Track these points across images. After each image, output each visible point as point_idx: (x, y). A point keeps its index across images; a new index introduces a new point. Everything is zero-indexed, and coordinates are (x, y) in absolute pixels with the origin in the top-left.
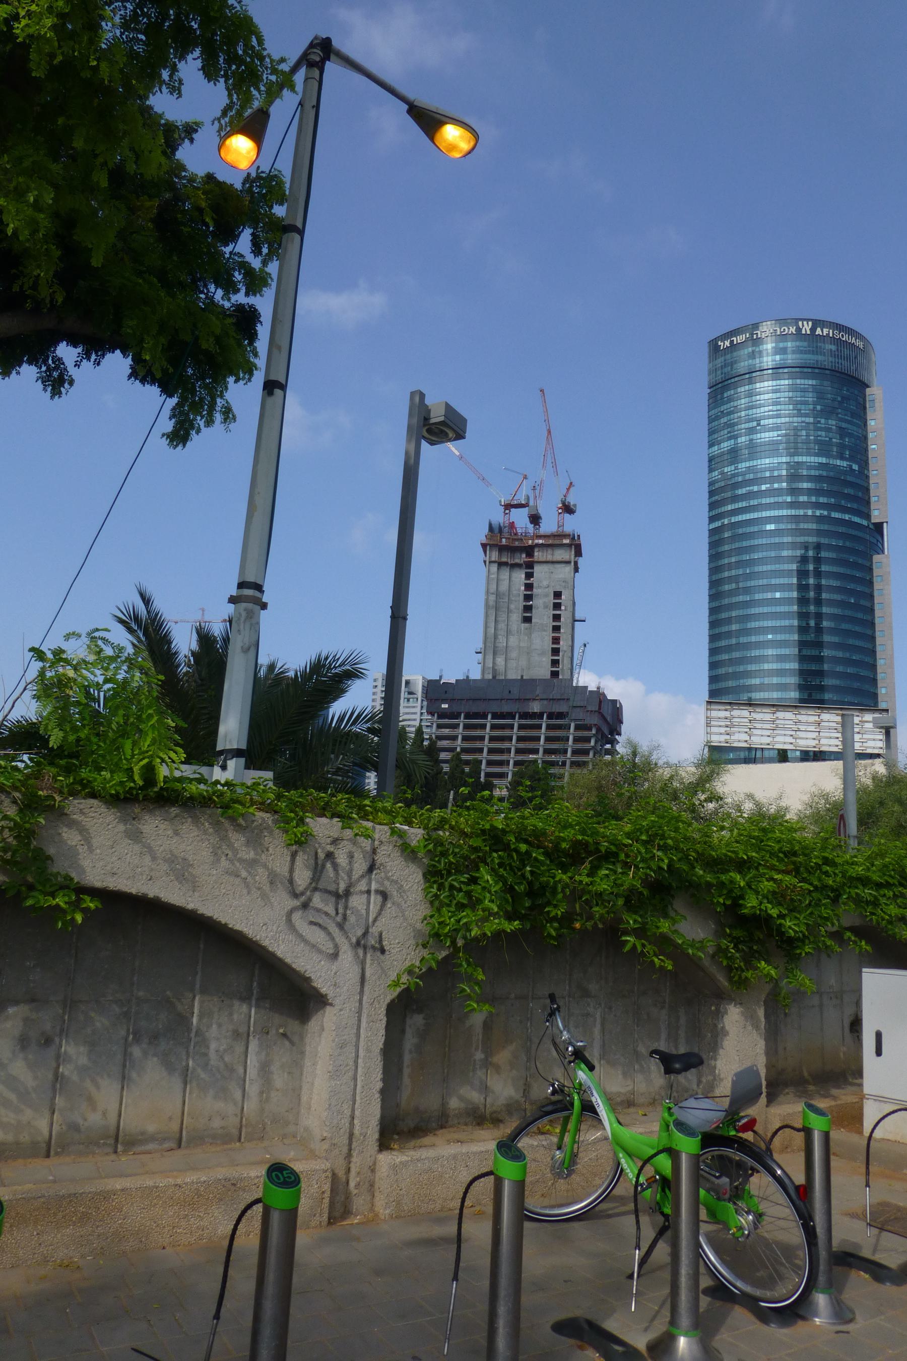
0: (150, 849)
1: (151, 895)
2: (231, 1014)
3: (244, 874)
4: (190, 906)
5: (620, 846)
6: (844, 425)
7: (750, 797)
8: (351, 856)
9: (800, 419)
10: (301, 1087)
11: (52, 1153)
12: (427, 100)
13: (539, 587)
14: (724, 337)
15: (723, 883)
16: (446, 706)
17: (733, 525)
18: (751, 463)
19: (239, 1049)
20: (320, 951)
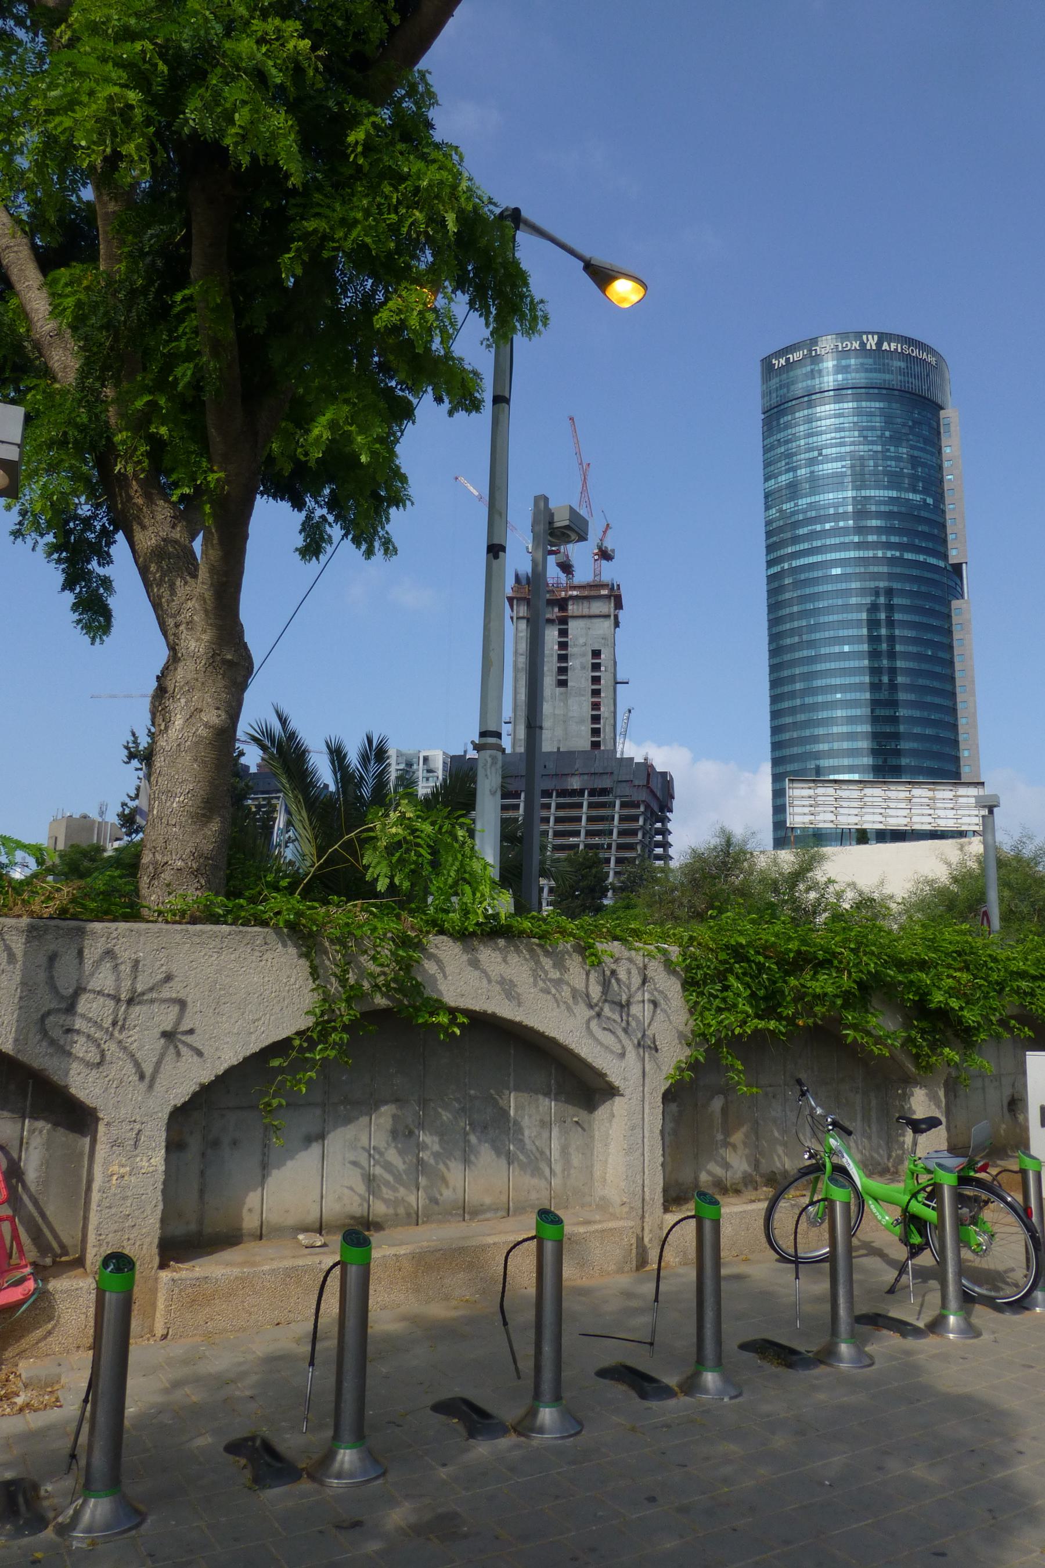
0: (484, 972)
1: (489, 1012)
2: (537, 1107)
3: (553, 991)
4: (518, 1019)
5: (834, 955)
6: (916, 453)
7: (852, 885)
8: (629, 972)
9: (866, 448)
10: (592, 1165)
11: (420, 1221)
12: (600, 258)
13: (575, 645)
14: (779, 354)
15: (912, 982)
17: (794, 570)
18: (813, 499)
19: (545, 1135)
20: (612, 1052)
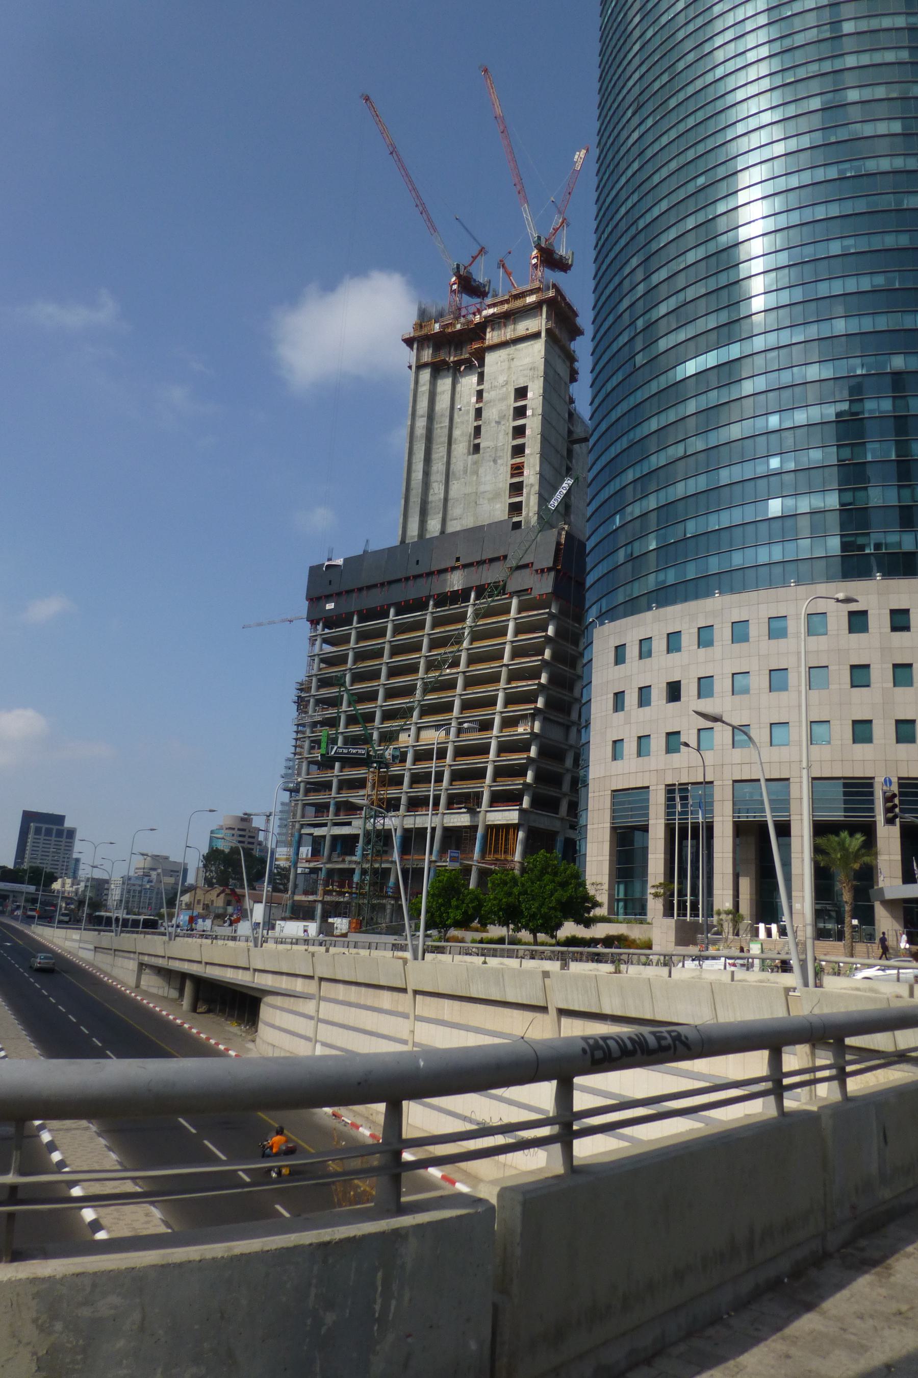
13: (493, 388)
16: (330, 606)
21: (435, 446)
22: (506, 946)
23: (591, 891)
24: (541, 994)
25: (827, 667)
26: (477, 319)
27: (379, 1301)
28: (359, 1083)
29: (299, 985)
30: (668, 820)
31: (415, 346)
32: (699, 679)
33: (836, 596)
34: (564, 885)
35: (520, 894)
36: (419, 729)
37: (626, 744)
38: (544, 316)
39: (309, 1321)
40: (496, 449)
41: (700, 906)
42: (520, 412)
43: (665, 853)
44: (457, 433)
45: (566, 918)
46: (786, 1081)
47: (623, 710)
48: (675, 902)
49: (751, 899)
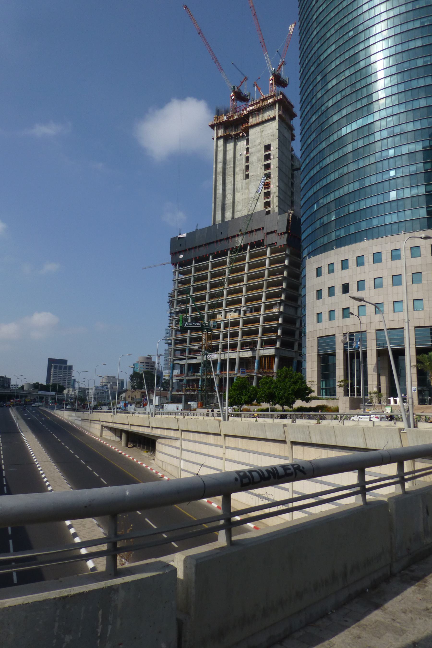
13: (254, 146)
16: (181, 256)
21: (227, 177)
22: (270, 413)
23: (309, 385)
24: (283, 435)
25: (421, 272)
26: (245, 112)
27: (100, 627)
28: (86, 507)
29: (172, 434)
30: (345, 350)
31: (215, 128)
32: (358, 282)
33: (421, 236)
34: (295, 383)
35: (275, 388)
36: (226, 313)
37: (323, 315)
38: (277, 109)
39: (54, 641)
40: (256, 176)
41: (361, 390)
42: (267, 157)
43: (344, 366)
44: (237, 169)
45: (297, 399)
46: (367, 486)
47: (321, 298)
48: (349, 389)
49: (386, 386)
